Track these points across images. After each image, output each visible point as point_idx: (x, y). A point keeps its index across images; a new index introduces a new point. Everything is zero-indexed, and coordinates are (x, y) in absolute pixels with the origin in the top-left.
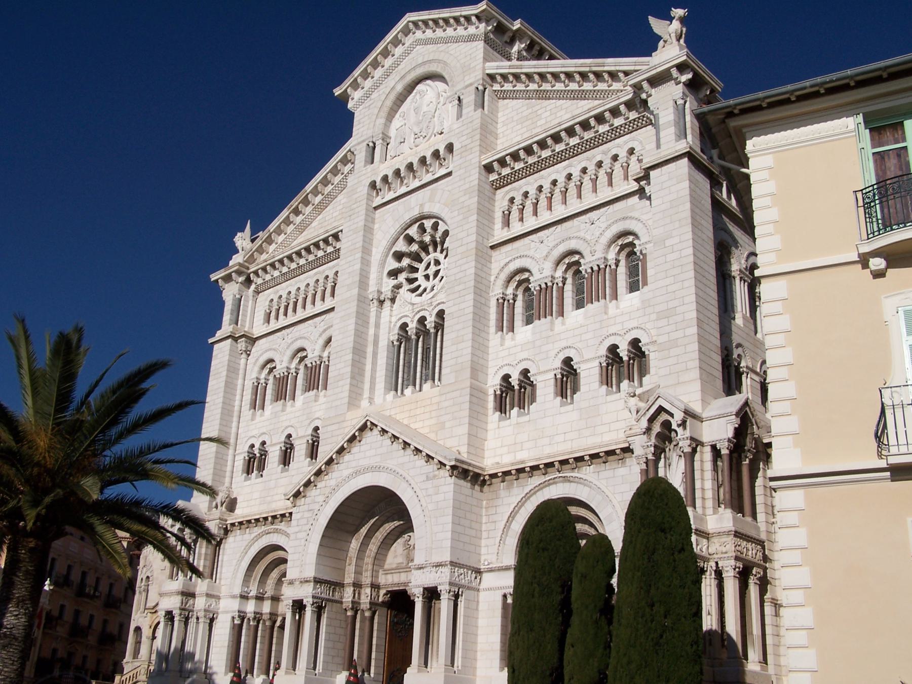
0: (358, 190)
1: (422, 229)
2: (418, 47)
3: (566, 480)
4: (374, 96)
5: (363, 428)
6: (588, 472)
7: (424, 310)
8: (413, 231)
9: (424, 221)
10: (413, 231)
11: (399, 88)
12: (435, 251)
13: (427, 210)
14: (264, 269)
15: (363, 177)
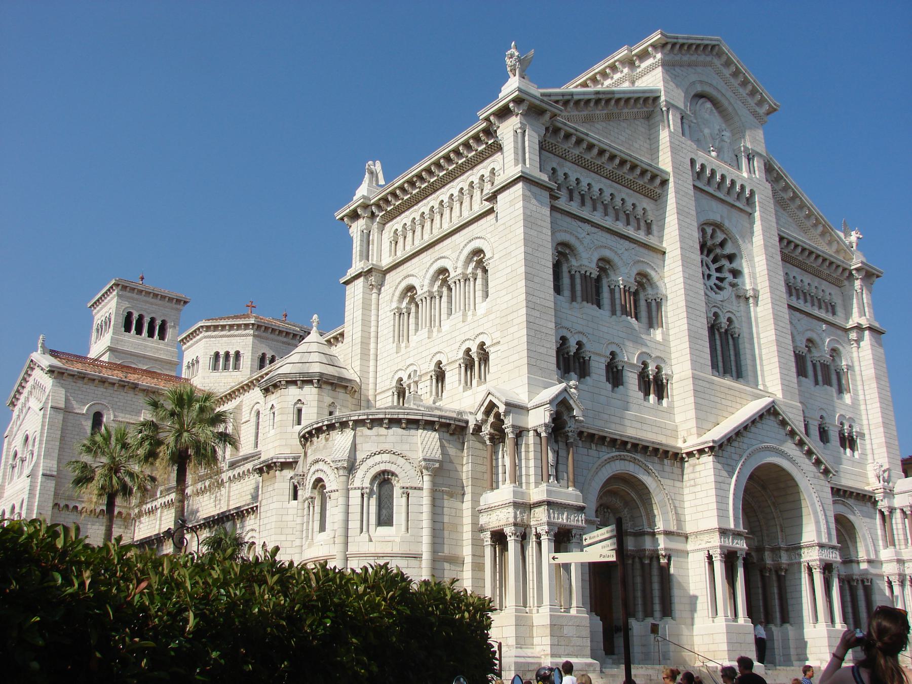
0: (681, 154)
1: (712, 237)
2: (710, 68)
3: (844, 504)
4: (677, 69)
5: (768, 411)
6: (851, 502)
7: (719, 308)
8: (709, 231)
9: (718, 230)
10: (709, 231)
11: (699, 88)
12: (708, 256)
13: (727, 224)
14: (568, 136)
15: (683, 146)
